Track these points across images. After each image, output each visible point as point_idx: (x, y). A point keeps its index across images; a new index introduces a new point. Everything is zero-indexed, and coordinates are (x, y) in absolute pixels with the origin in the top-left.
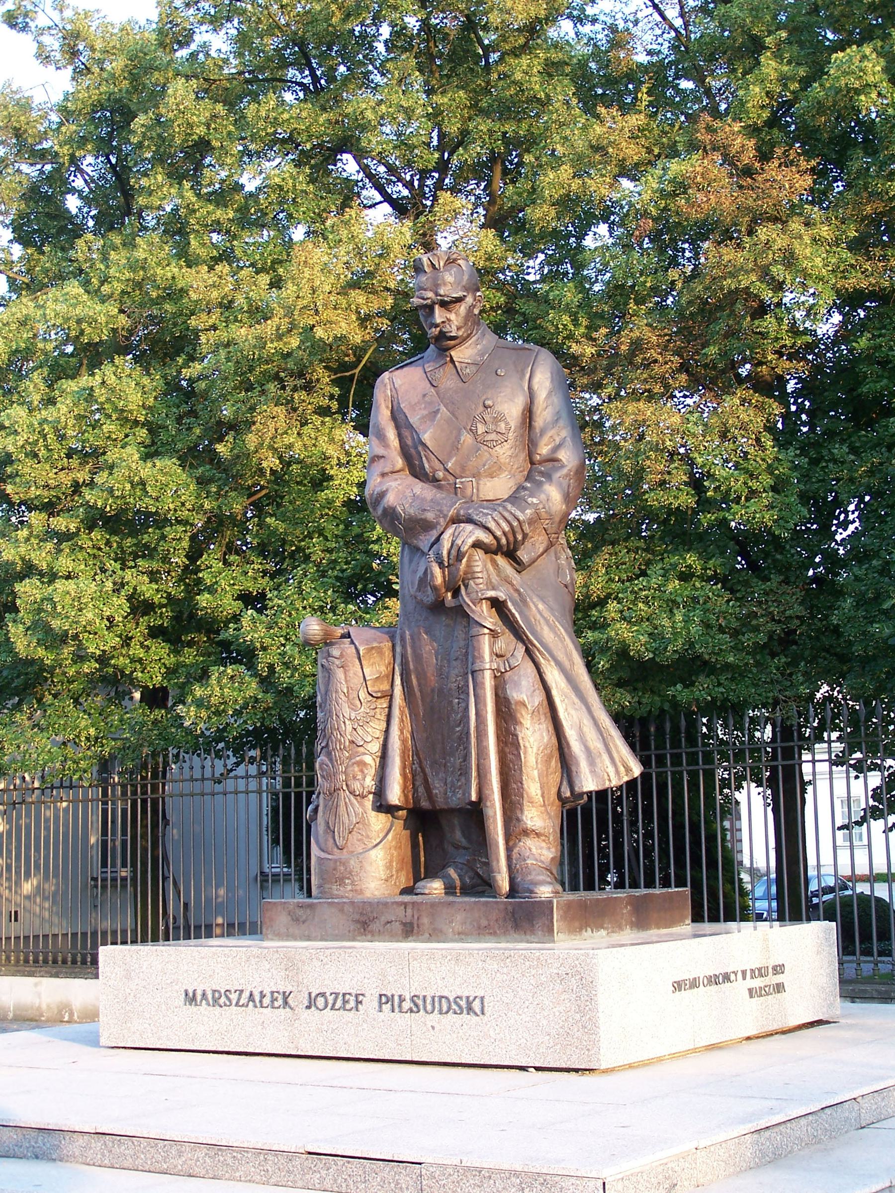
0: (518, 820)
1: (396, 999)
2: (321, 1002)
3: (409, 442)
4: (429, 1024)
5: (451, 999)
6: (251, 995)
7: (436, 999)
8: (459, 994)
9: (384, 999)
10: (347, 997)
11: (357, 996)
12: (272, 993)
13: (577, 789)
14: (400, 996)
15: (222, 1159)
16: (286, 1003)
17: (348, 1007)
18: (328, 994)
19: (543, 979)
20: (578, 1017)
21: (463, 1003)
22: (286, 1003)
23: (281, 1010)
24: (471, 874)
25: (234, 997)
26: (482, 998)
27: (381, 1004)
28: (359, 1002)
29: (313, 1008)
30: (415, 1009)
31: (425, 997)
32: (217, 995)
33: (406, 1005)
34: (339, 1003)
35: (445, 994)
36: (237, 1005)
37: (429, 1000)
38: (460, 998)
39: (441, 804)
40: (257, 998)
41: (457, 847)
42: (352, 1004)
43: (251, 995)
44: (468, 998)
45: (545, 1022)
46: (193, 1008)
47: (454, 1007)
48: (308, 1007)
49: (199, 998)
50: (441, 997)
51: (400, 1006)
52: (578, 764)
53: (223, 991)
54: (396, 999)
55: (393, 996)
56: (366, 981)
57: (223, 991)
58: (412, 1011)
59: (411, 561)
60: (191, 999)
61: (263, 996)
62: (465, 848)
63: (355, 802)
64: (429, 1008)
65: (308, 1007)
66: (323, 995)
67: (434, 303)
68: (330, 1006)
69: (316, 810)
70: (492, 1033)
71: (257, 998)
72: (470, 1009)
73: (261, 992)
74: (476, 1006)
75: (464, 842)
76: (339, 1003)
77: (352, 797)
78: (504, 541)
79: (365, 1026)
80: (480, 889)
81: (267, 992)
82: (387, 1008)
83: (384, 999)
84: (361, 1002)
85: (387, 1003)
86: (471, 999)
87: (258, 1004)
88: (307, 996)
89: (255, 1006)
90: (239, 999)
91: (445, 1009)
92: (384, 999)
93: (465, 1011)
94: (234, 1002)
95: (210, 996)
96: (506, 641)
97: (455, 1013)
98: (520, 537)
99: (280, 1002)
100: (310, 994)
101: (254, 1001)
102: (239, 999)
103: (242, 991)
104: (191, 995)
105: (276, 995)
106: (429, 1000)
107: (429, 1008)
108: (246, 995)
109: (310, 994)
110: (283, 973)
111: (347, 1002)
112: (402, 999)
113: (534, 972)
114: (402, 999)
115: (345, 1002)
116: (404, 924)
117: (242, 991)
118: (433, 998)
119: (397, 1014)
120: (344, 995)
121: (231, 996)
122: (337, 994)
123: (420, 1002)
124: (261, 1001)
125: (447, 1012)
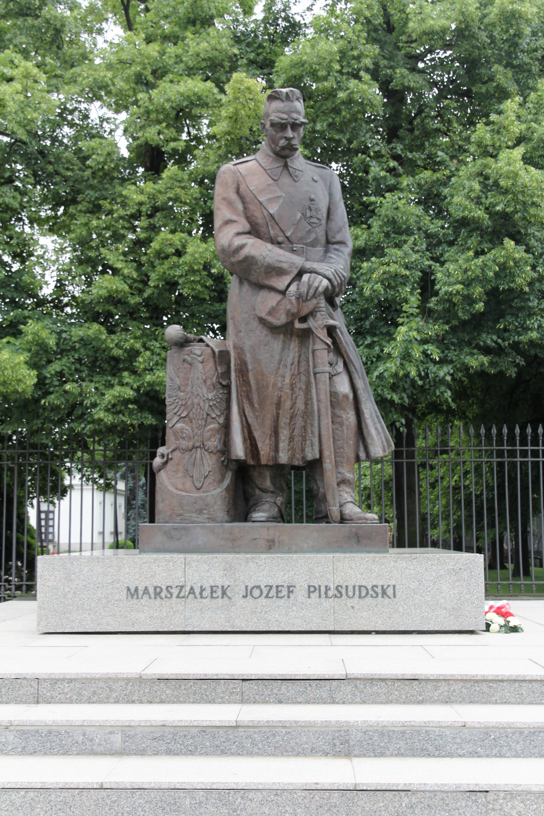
1: (323, 589)
2: (256, 593)
3: (258, 214)
4: (349, 605)
5: (369, 587)
6: (192, 588)
7: (357, 588)
8: (374, 583)
9: (312, 589)
10: (280, 588)
11: (289, 587)
12: (212, 587)
13: (372, 455)
14: (326, 587)
15: (477, 689)
16: (224, 593)
17: (280, 595)
18: (263, 587)
19: (442, 572)
20: (468, 597)
21: (379, 590)
22: (224, 593)
23: (220, 600)
25: (175, 592)
26: (394, 586)
27: (309, 592)
28: (289, 592)
29: (249, 597)
30: (339, 595)
31: (347, 587)
32: (158, 590)
33: (330, 593)
34: (273, 592)
35: (364, 584)
36: (178, 597)
37: (350, 588)
38: (377, 587)
40: (197, 591)
42: (285, 592)
43: (192, 588)
44: (382, 586)
45: (443, 601)
46: (135, 601)
47: (371, 592)
48: (245, 597)
49: (141, 593)
50: (360, 587)
51: (326, 593)
52: (373, 439)
53: (164, 588)
54: (323, 589)
55: (320, 587)
56: (296, 576)
57: (164, 588)
58: (336, 596)
60: (133, 593)
61: (202, 590)
62: (272, 492)
63: (208, 456)
64: (350, 594)
65: (245, 597)
66: (258, 587)
67: (289, 123)
68: (264, 595)
70: (401, 609)
71: (197, 591)
72: (384, 593)
73: (201, 587)
74: (390, 591)
75: (272, 489)
76: (273, 592)
77: (206, 453)
79: (295, 608)
81: (207, 585)
82: (315, 595)
83: (312, 589)
84: (292, 591)
85: (314, 592)
86: (385, 587)
87: (198, 596)
88: (244, 589)
89: (196, 598)
90: (179, 593)
91: (363, 594)
92: (311, 590)
93: (380, 596)
94: (175, 595)
95: (151, 590)
96: (332, 357)
97: (372, 596)
99: (219, 593)
100: (247, 587)
101: (194, 593)
102: (179, 593)
103: (182, 587)
104: (132, 591)
105: (215, 589)
106: (350, 588)
107: (350, 594)
108: (188, 589)
109: (247, 587)
110: (221, 573)
111: (281, 591)
112: (327, 589)
113: (434, 568)
114: (327, 589)
115: (278, 592)
116: (268, 541)
117: (182, 587)
118: (354, 587)
119: (323, 599)
120: (277, 587)
121: (172, 591)
122: (271, 587)
123: (344, 591)
124: (201, 593)
125: (366, 596)
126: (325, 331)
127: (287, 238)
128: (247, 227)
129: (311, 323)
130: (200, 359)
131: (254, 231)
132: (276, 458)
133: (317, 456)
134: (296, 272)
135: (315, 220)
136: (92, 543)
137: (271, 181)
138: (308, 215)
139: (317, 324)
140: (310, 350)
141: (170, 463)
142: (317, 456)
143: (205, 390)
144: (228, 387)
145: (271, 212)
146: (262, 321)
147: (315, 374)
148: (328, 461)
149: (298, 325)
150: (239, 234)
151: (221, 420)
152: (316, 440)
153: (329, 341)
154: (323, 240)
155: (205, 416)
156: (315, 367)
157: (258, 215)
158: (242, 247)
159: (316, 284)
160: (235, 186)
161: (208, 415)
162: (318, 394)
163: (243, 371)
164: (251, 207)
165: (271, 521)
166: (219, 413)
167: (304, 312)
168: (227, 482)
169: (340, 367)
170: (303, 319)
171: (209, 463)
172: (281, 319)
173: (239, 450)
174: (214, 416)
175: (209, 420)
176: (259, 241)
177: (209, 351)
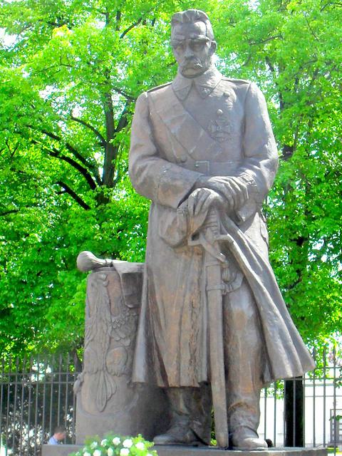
0: (235, 396)
24: (190, 432)
39: (172, 381)
41: (180, 414)
59: (159, 217)
63: (110, 379)
69: (81, 384)
78: (232, 203)
80: (195, 443)
98: (242, 200)
126: (217, 246)
127: (190, 155)
128: (153, 149)
129: (201, 241)
130: (104, 283)
131: (159, 153)
132: (179, 379)
133: (205, 378)
134: (189, 188)
135: (222, 135)
136: (314, 443)
137: (177, 102)
138: (213, 130)
139: (208, 242)
140: (205, 268)
141: (84, 385)
142: (205, 378)
143: (108, 315)
144: (137, 307)
145: (173, 132)
146: (163, 239)
147: (206, 292)
148: (216, 383)
149: (191, 243)
150: (144, 157)
151: (128, 342)
152: (204, 360)
153: (221, 257)
154: (237, 153)
155: (108, 339)
156: (207, 285)
157: (163, 136)
158: (142, 170)
159: (203, 199)
160: (145, 112)
161: (111, 338)
162: (208, 313)
163: (151, 292)
164: (158, 129)
165: (170, 445)
166: (123, 336)
167: (194, 228)
168: (134, 404)
169: (239, 282)
170: (195, 237)
171: (114, 384)
172: (177, 238)
173: (140, 374)
174: (118, 339)
175: (114, 343)
176: (162, 161)
177: (113, 275)
